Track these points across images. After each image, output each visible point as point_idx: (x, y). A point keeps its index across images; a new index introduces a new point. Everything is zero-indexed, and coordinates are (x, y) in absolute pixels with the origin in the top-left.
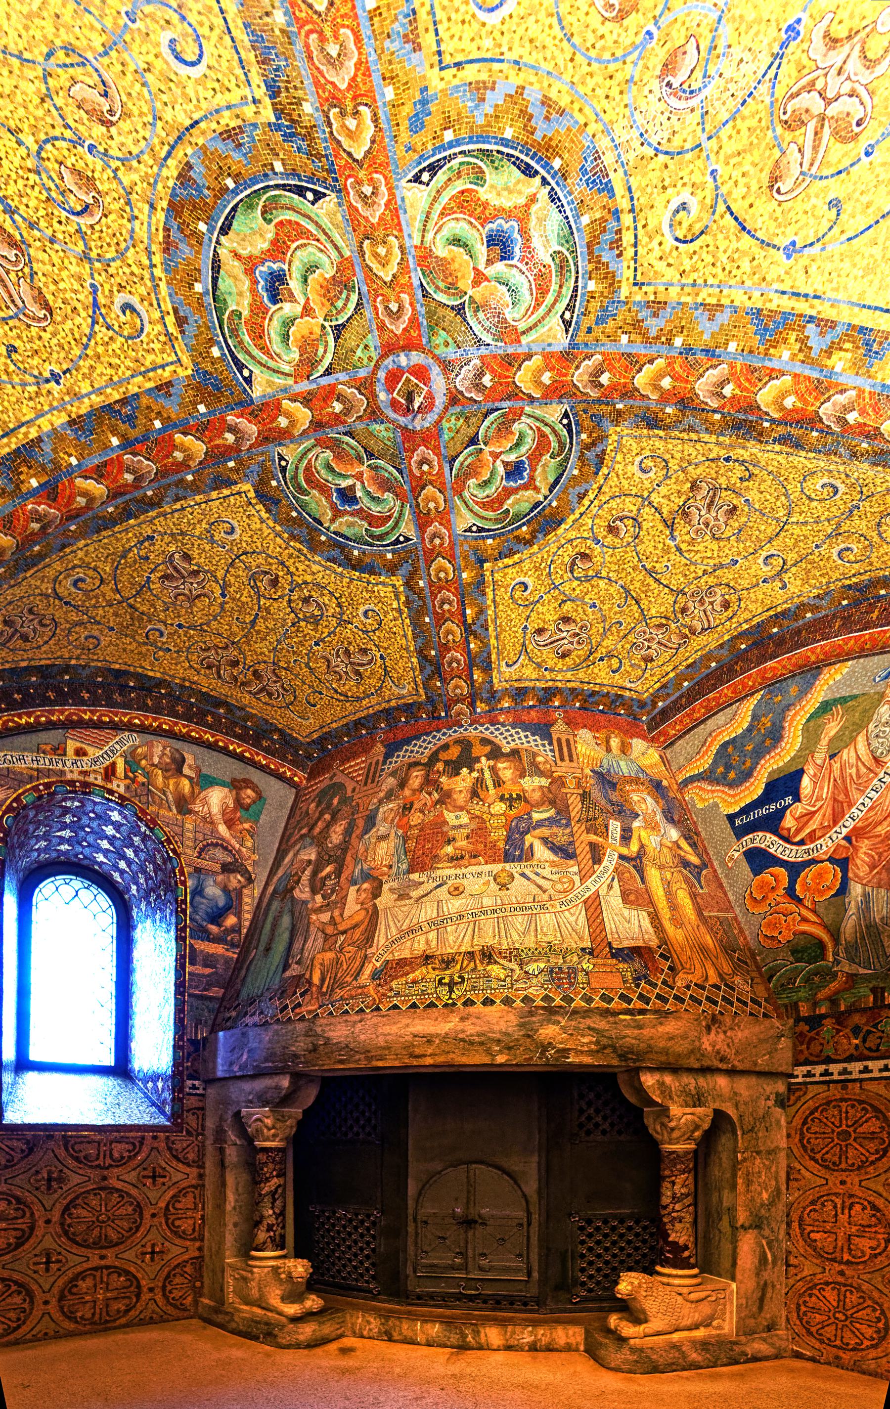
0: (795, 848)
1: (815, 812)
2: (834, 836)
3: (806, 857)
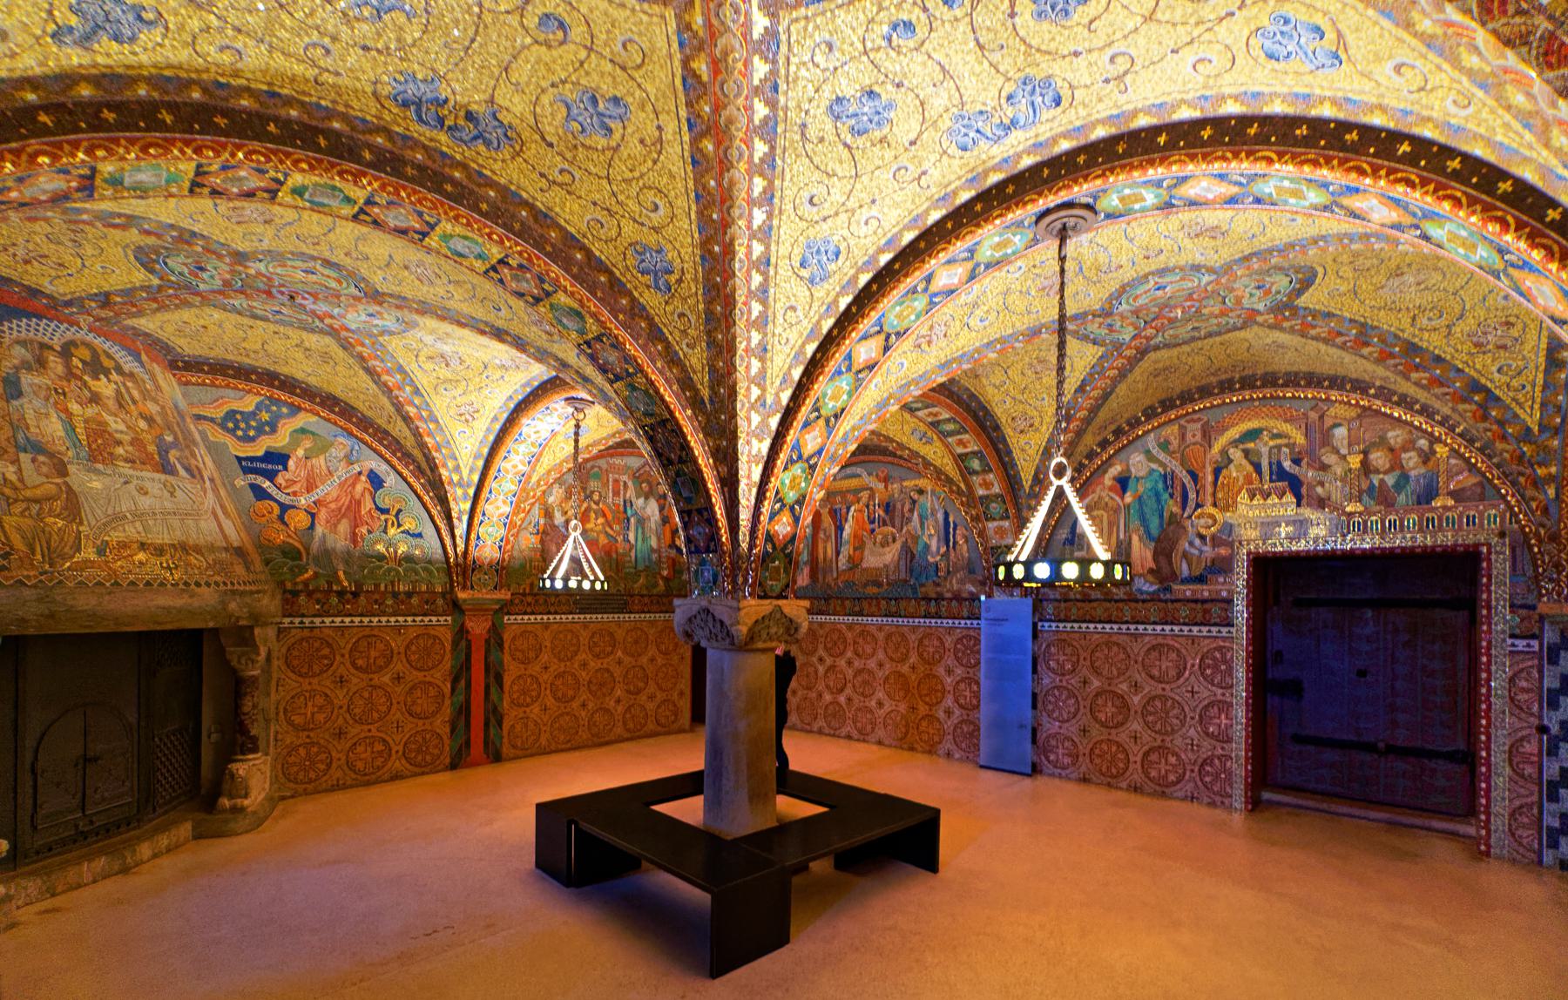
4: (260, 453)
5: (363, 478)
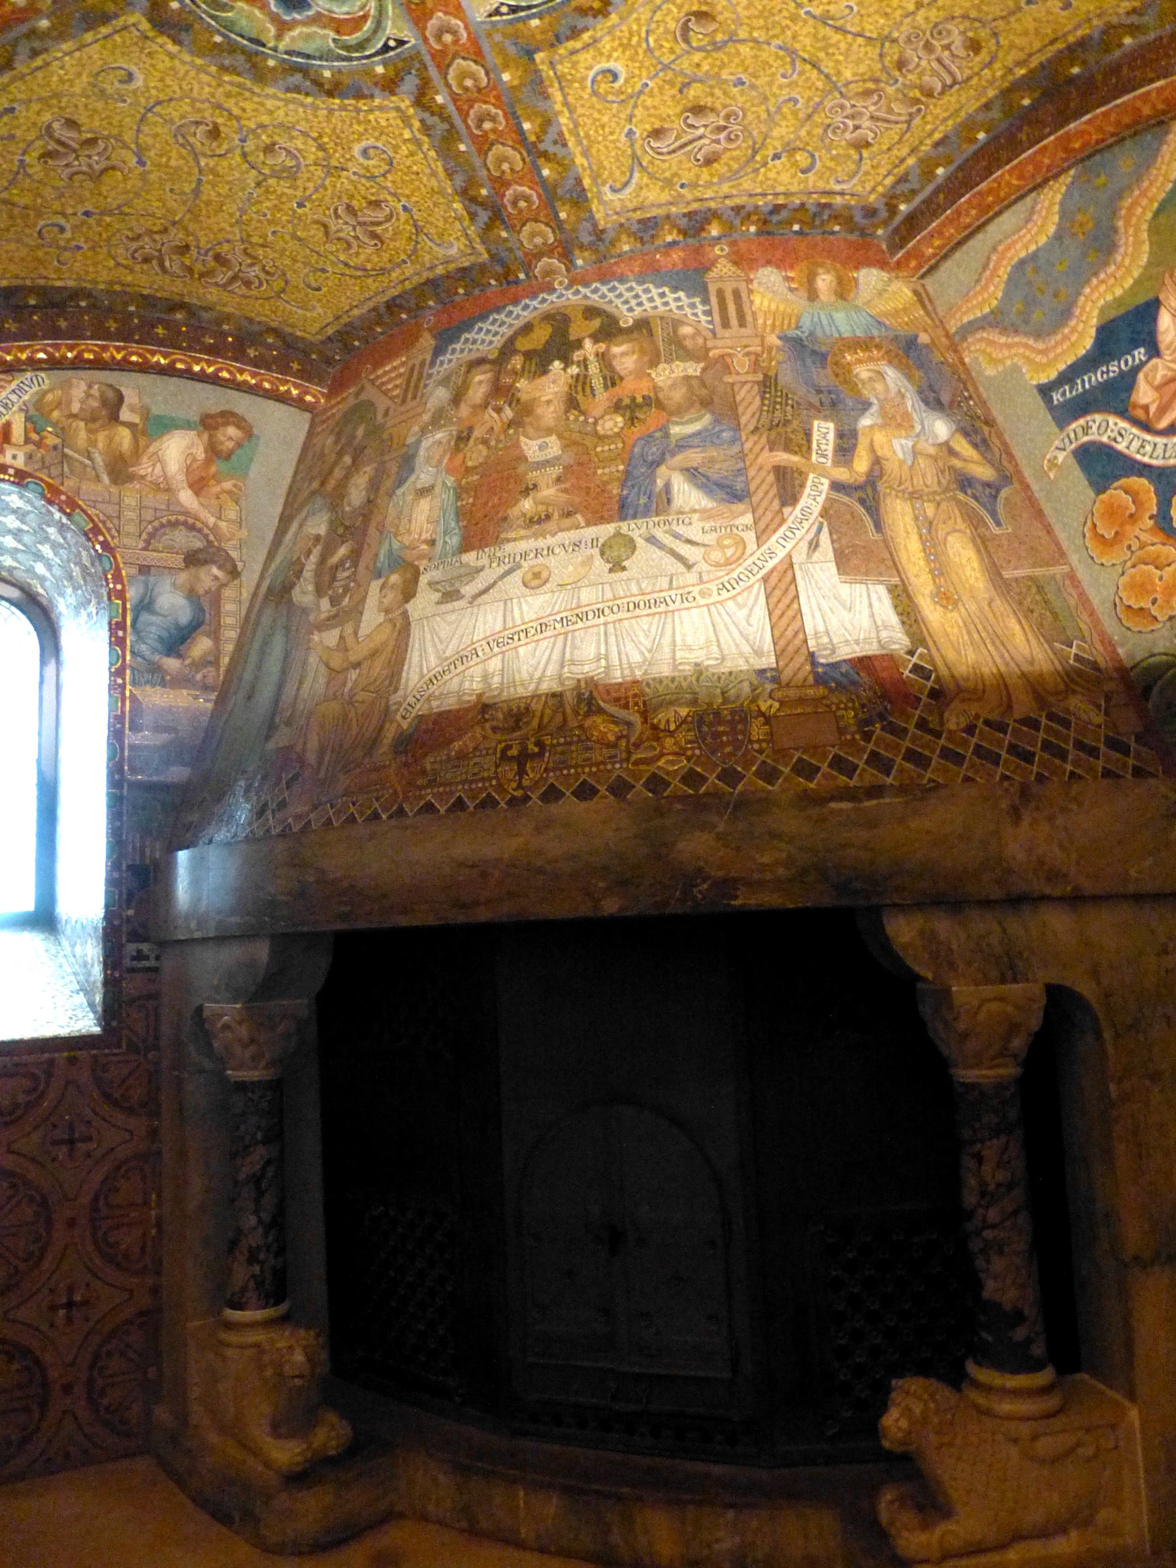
0: (1160, 440)
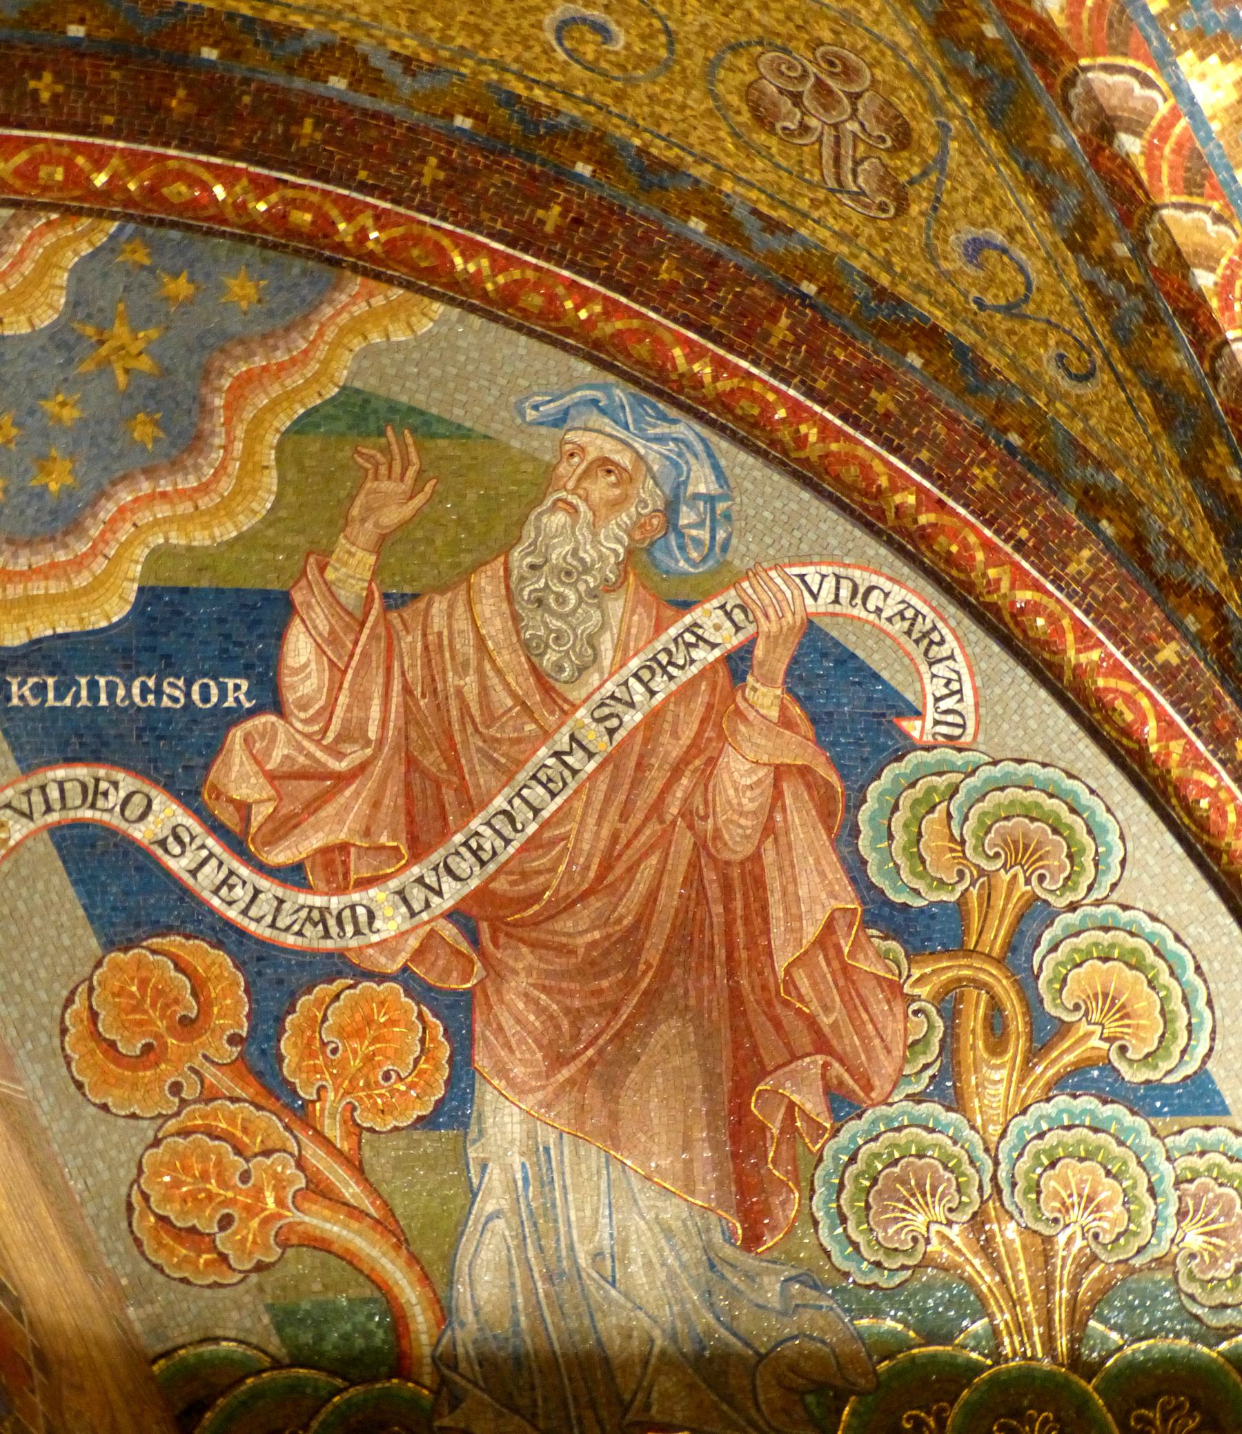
1: (343, 779)
2: (417, 896)
3: (312, 939)
4: (114, 608)
5: (765, 696)
